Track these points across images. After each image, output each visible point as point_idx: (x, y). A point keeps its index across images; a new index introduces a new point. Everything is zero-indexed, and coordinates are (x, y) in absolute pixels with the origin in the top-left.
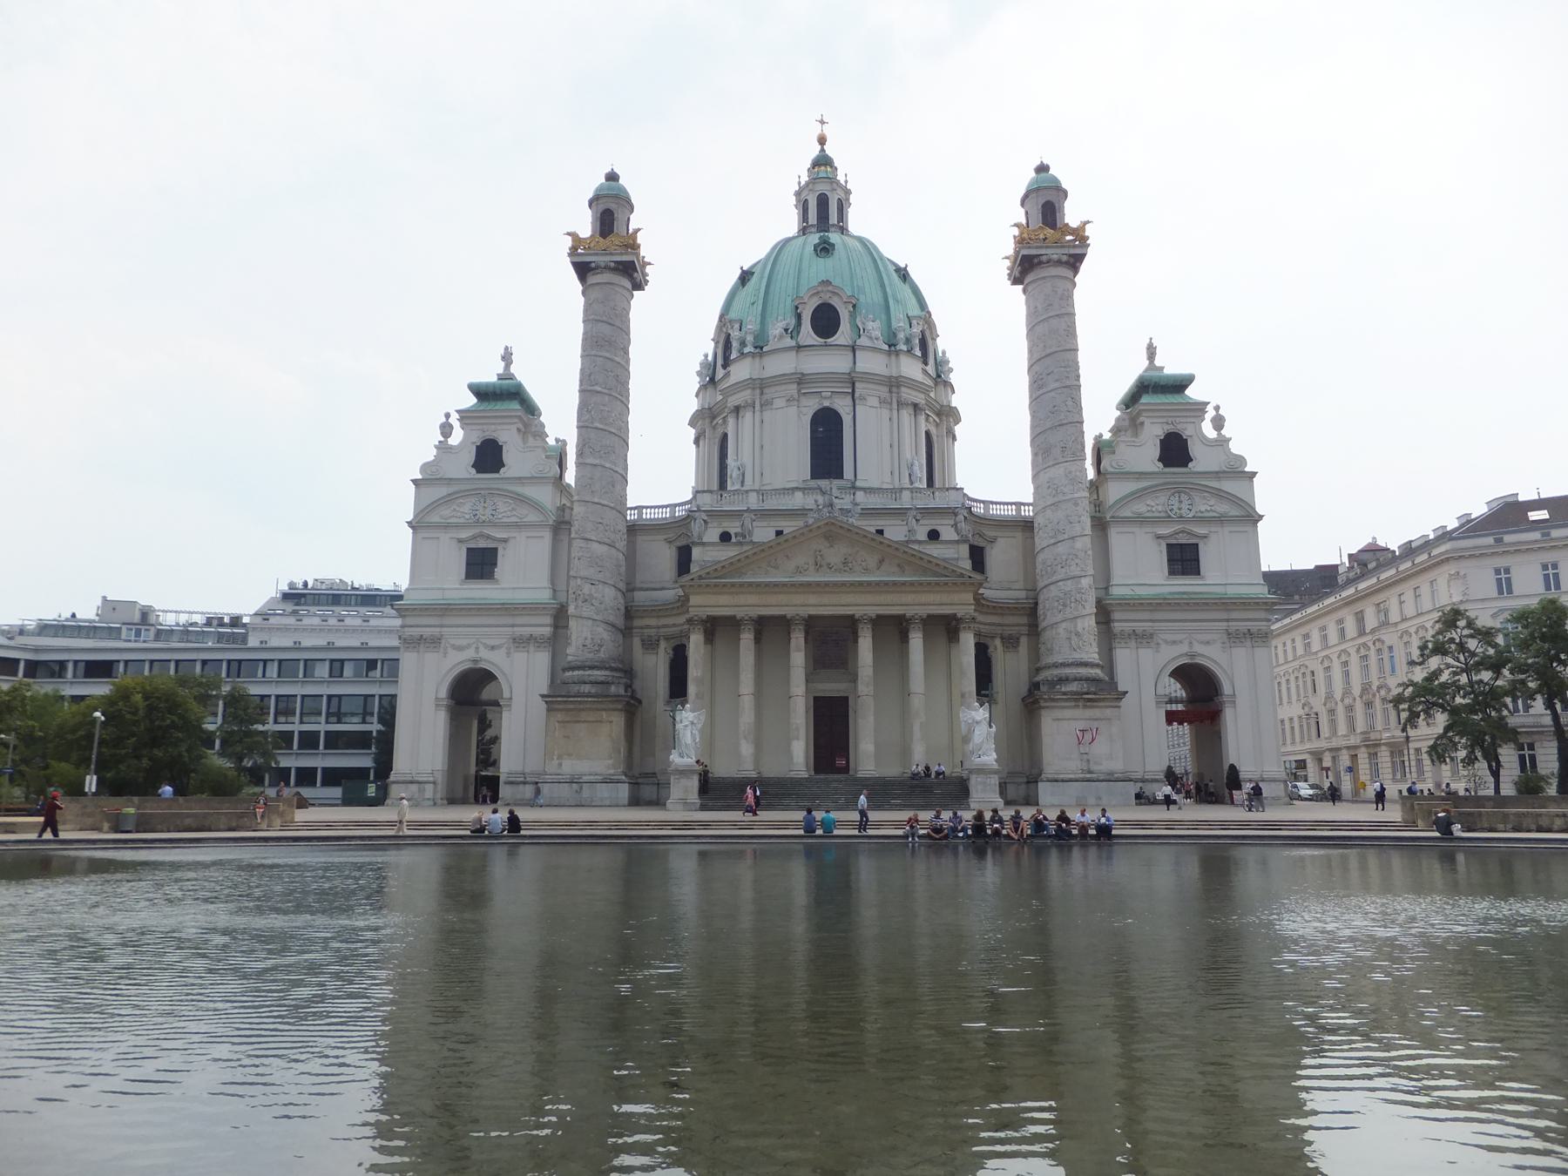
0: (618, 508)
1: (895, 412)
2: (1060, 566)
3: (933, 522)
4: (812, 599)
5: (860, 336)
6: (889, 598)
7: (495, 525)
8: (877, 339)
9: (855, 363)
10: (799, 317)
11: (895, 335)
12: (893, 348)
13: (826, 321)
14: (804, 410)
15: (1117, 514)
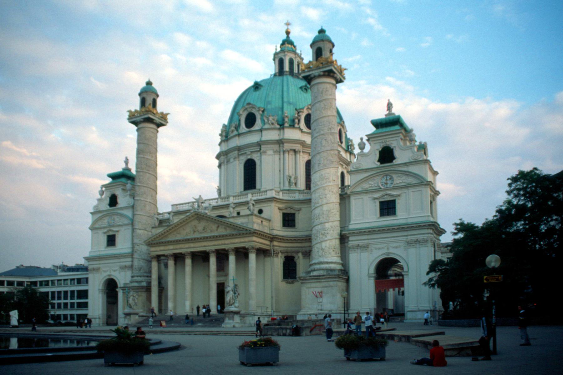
0: (147, 215)
1: (282, 156)
2: (316, 219)
3: (259, 206)
4: (192, 245)
5: (265, 124)
6: (220, 242)
7: (114, 226)
8: (273, 124)
9: (262, 136)
10: (240, 120)
11: (284, 120)
12: (282, 127)
13: (251, 120)
14: (241, 161)
15: (352, 191)
